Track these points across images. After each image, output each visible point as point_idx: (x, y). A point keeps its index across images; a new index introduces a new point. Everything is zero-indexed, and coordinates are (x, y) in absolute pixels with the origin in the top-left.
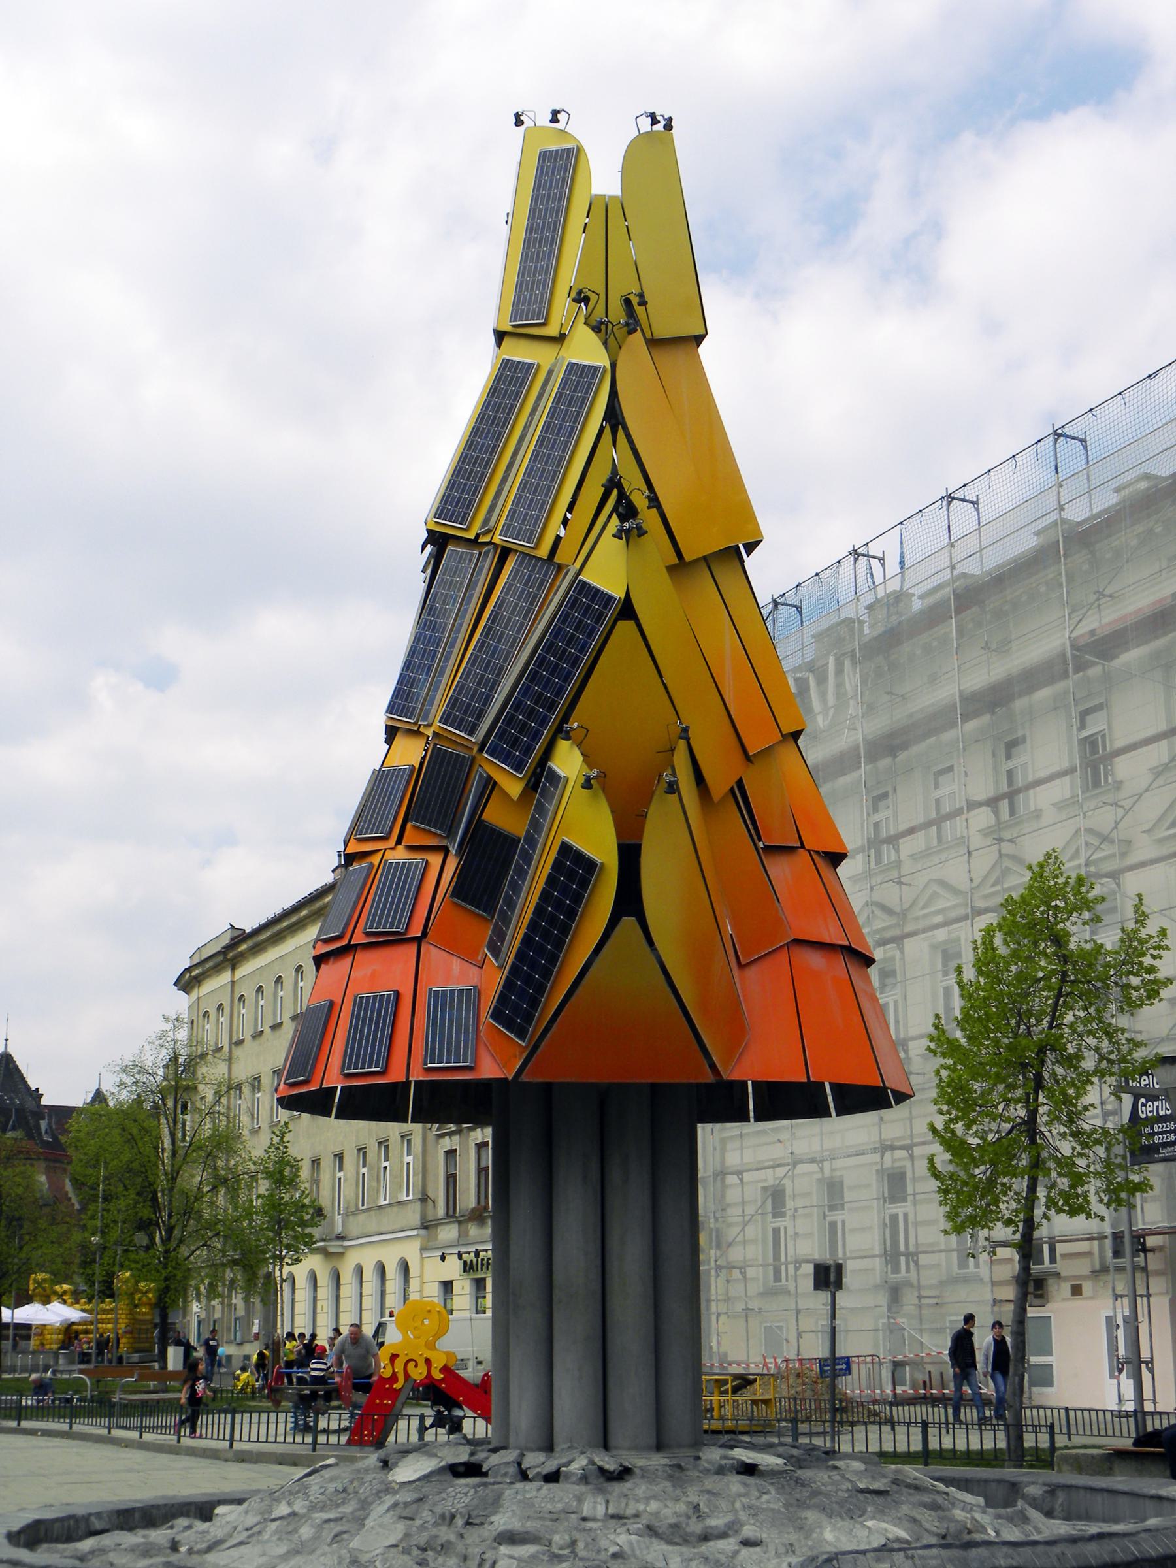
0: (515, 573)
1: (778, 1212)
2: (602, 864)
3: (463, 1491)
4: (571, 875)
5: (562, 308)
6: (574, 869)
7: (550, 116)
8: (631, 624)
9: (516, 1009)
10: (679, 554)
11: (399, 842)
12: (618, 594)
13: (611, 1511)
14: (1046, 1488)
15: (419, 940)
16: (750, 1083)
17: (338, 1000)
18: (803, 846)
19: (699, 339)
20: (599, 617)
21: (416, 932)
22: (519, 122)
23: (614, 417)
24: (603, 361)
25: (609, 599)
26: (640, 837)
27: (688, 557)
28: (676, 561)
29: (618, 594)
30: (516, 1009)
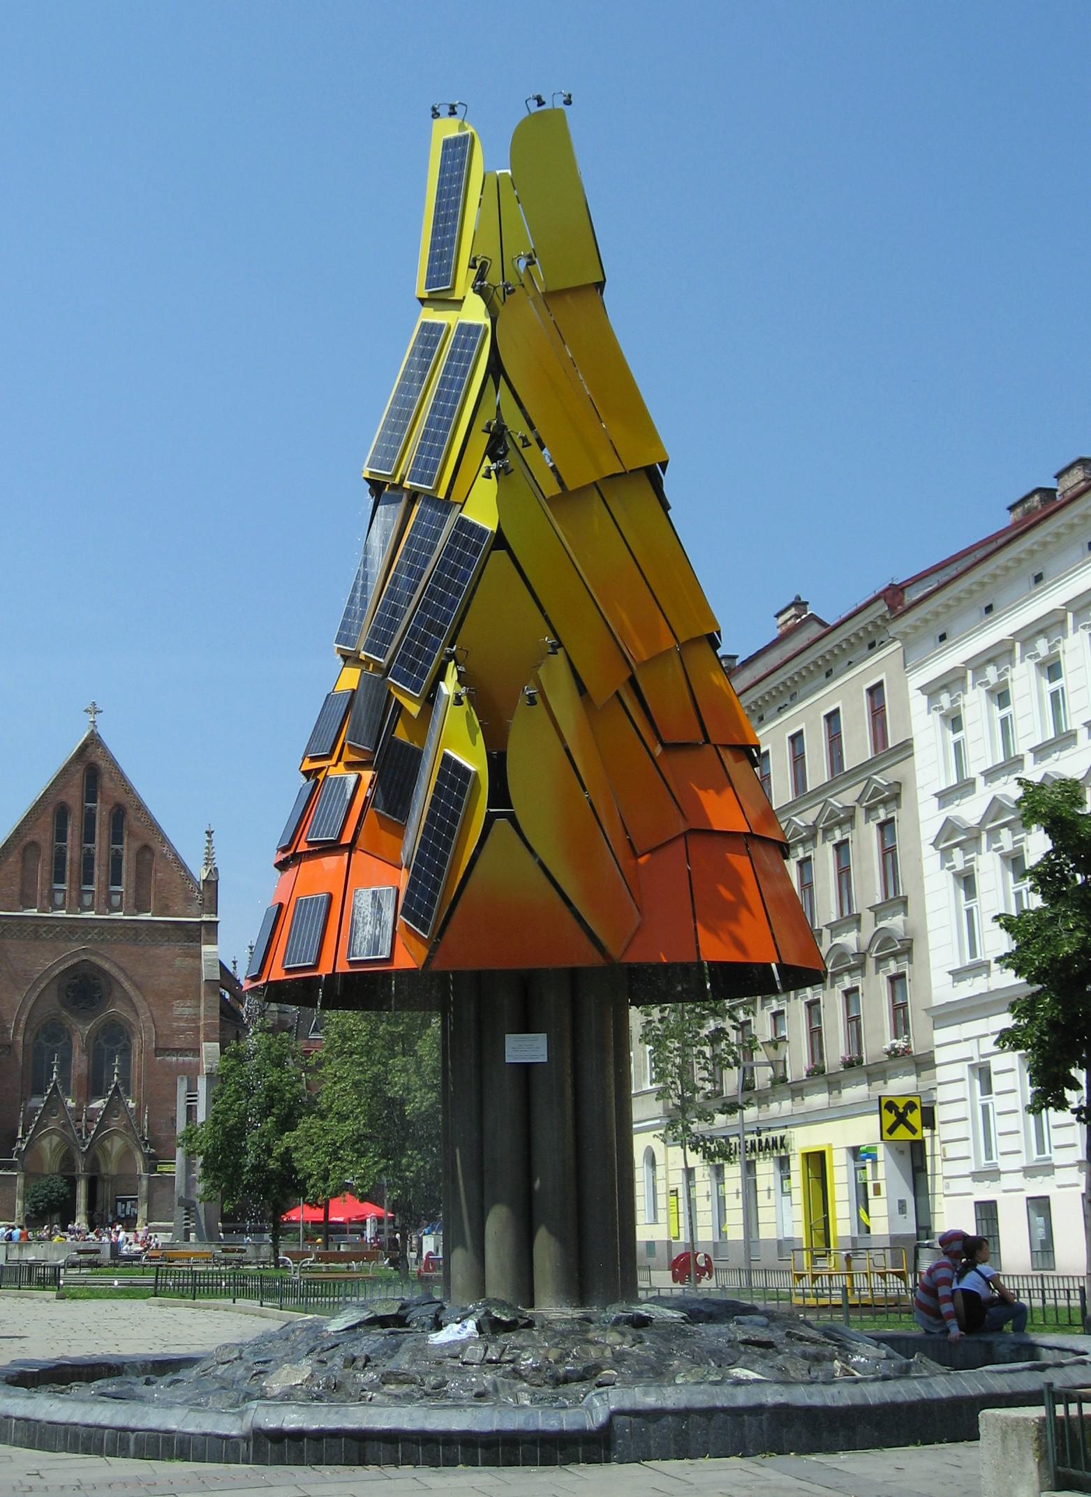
0: (421, 515)
1: (987, 1089)
2: (476, 773)
3: (374, 1340)
4: (452, 784)
5: (464, 277)
6: (453, 773)
7: (431, 113)
8: (503, 553)
9: (419, 905)
10: (561, 483)
11: (339, 760)
12: (491, 527)
13: (488, 1357)
14: (1013, 1347)
15: (351, 847)
16: (774, 966)
17: (286, 903)
18: (707, 741)
19: (600, 286)
20: (476, 550)
21: (347, 839)
22: (568, 102)
23: (496, 369)
24: (488, 322)
25: (483, 532)
26: (910, 730)
27: (571, 486)
28: (558, 490)
29: (491, 527)
30: (419, 905)
